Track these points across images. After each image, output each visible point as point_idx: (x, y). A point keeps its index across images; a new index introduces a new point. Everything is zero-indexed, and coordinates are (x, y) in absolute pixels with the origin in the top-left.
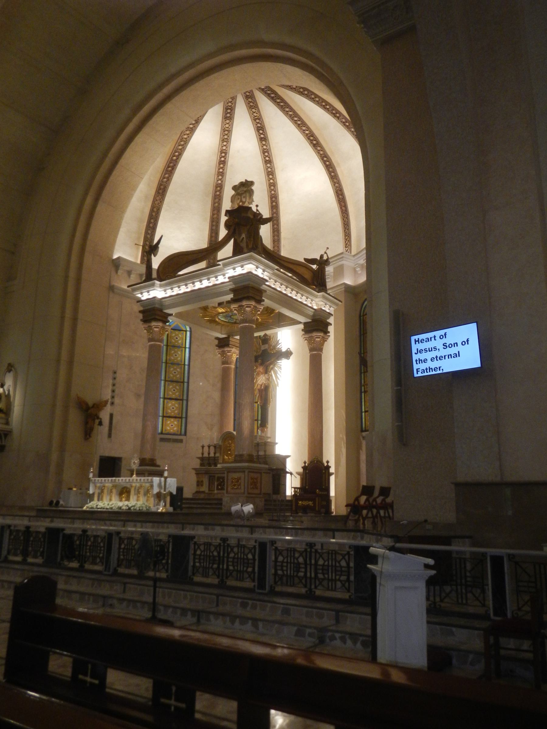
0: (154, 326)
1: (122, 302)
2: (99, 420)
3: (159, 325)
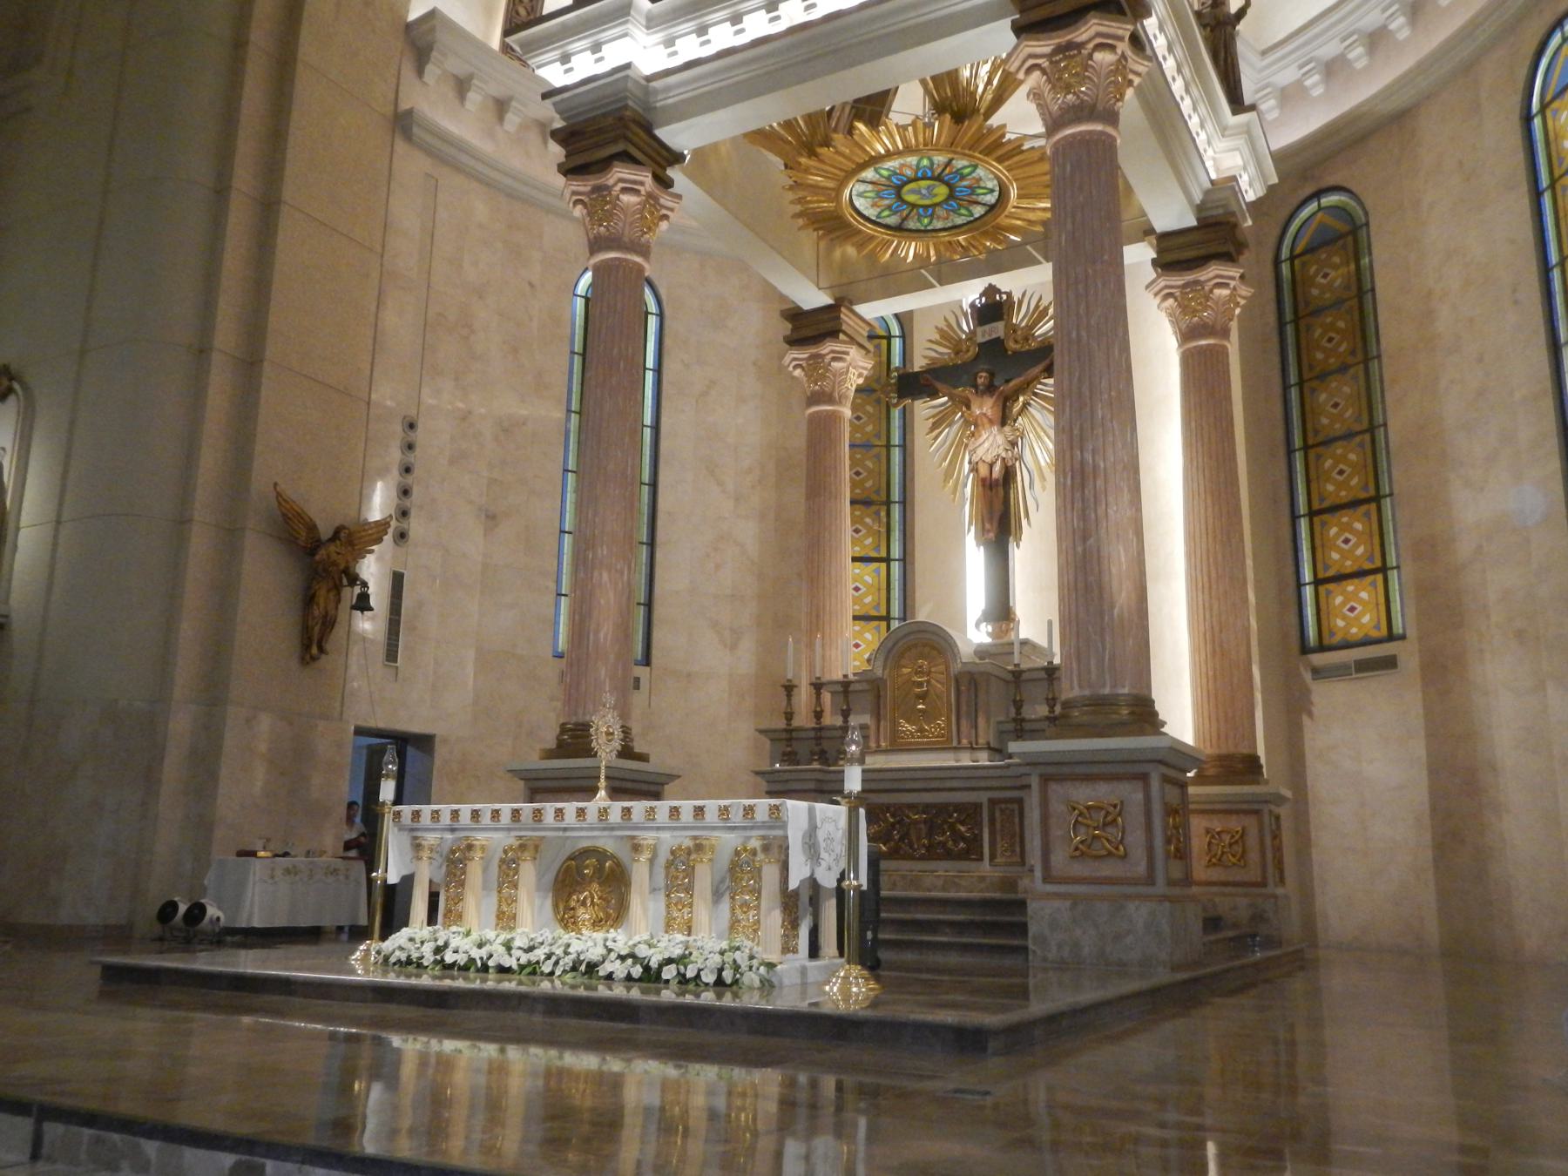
0: (621, 185)
1: (437, 181)
2: (357, 590)
3: (642, 183)
